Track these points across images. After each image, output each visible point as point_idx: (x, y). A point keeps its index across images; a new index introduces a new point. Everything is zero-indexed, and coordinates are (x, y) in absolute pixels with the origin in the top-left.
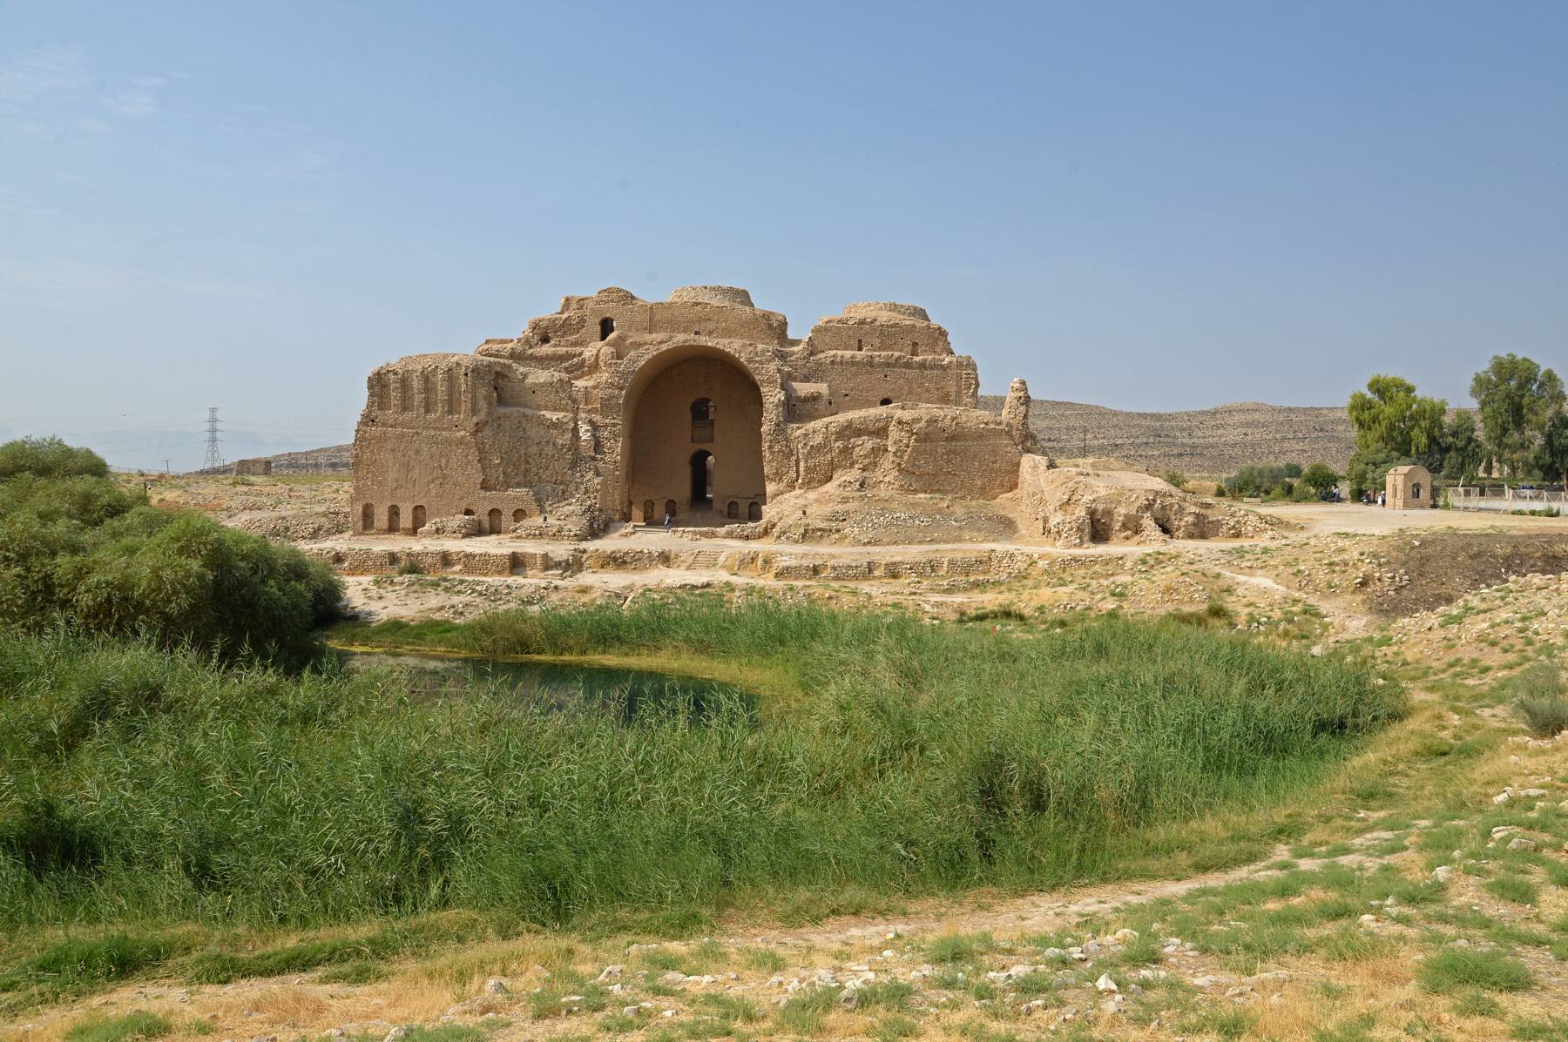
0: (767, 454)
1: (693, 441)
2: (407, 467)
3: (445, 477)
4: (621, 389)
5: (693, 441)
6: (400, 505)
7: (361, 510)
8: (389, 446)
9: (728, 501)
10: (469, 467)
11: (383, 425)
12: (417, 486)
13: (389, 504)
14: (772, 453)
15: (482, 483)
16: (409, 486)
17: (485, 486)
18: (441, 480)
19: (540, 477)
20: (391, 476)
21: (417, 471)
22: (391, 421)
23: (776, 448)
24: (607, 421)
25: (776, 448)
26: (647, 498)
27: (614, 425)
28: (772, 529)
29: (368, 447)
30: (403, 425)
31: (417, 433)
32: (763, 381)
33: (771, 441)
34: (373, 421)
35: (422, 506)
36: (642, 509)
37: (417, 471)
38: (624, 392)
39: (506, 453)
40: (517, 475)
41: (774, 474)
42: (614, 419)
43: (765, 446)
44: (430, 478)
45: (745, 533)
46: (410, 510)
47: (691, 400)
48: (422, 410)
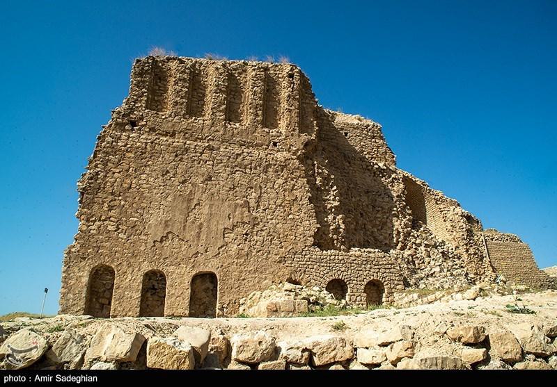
2: (189, 203)
3: (254, 223)
6: (165, 270)
7: (85, 280)
8: (158, 164)
10: (295, 209)
11: (152, 130)
12: (203, 236)
13: (146, 267)
15: (315, 236)
16: (190, 235)
17: (322, 241)
18: (247, 228)
20: (154, 219)
21: (206, 210)
22: (167, 127)
23: (472, 251)
25: (472, 251)
29: (118, 164)
30: (186, 133)
31: (211, 149)
34: (133, 124)
35: (212, 277)
37: (206, 210)
44: (228, 224)
46: (187, 280)
48: (221, 116)
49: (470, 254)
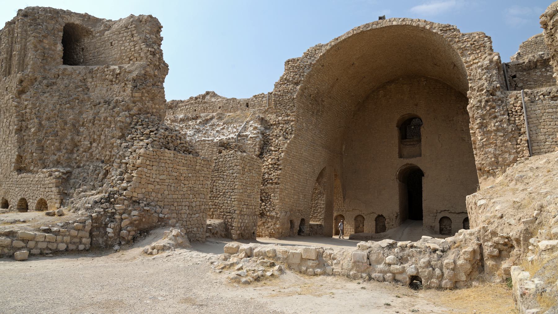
0: (477, 137)
1: (401, 156)
4: (297, 84)
5: (401, 156)
9: (440, 216)
14: (486, 133)
19: (91, 154)
23: (492, 126)
24: (280, 118)
26: (357, 213)
27: (287, 122)
28: (499, 257)
32: (465, 49)
33: (483, 117)
36: (353, 223)
38: (298, 87)
39: (48, 119)
40: (59, 150)
41: (491, 164)
42: (288, 115)
43: (474, 126)
45: (410, 269)
47: (397, 117)
49: (489, 132)
